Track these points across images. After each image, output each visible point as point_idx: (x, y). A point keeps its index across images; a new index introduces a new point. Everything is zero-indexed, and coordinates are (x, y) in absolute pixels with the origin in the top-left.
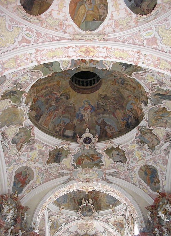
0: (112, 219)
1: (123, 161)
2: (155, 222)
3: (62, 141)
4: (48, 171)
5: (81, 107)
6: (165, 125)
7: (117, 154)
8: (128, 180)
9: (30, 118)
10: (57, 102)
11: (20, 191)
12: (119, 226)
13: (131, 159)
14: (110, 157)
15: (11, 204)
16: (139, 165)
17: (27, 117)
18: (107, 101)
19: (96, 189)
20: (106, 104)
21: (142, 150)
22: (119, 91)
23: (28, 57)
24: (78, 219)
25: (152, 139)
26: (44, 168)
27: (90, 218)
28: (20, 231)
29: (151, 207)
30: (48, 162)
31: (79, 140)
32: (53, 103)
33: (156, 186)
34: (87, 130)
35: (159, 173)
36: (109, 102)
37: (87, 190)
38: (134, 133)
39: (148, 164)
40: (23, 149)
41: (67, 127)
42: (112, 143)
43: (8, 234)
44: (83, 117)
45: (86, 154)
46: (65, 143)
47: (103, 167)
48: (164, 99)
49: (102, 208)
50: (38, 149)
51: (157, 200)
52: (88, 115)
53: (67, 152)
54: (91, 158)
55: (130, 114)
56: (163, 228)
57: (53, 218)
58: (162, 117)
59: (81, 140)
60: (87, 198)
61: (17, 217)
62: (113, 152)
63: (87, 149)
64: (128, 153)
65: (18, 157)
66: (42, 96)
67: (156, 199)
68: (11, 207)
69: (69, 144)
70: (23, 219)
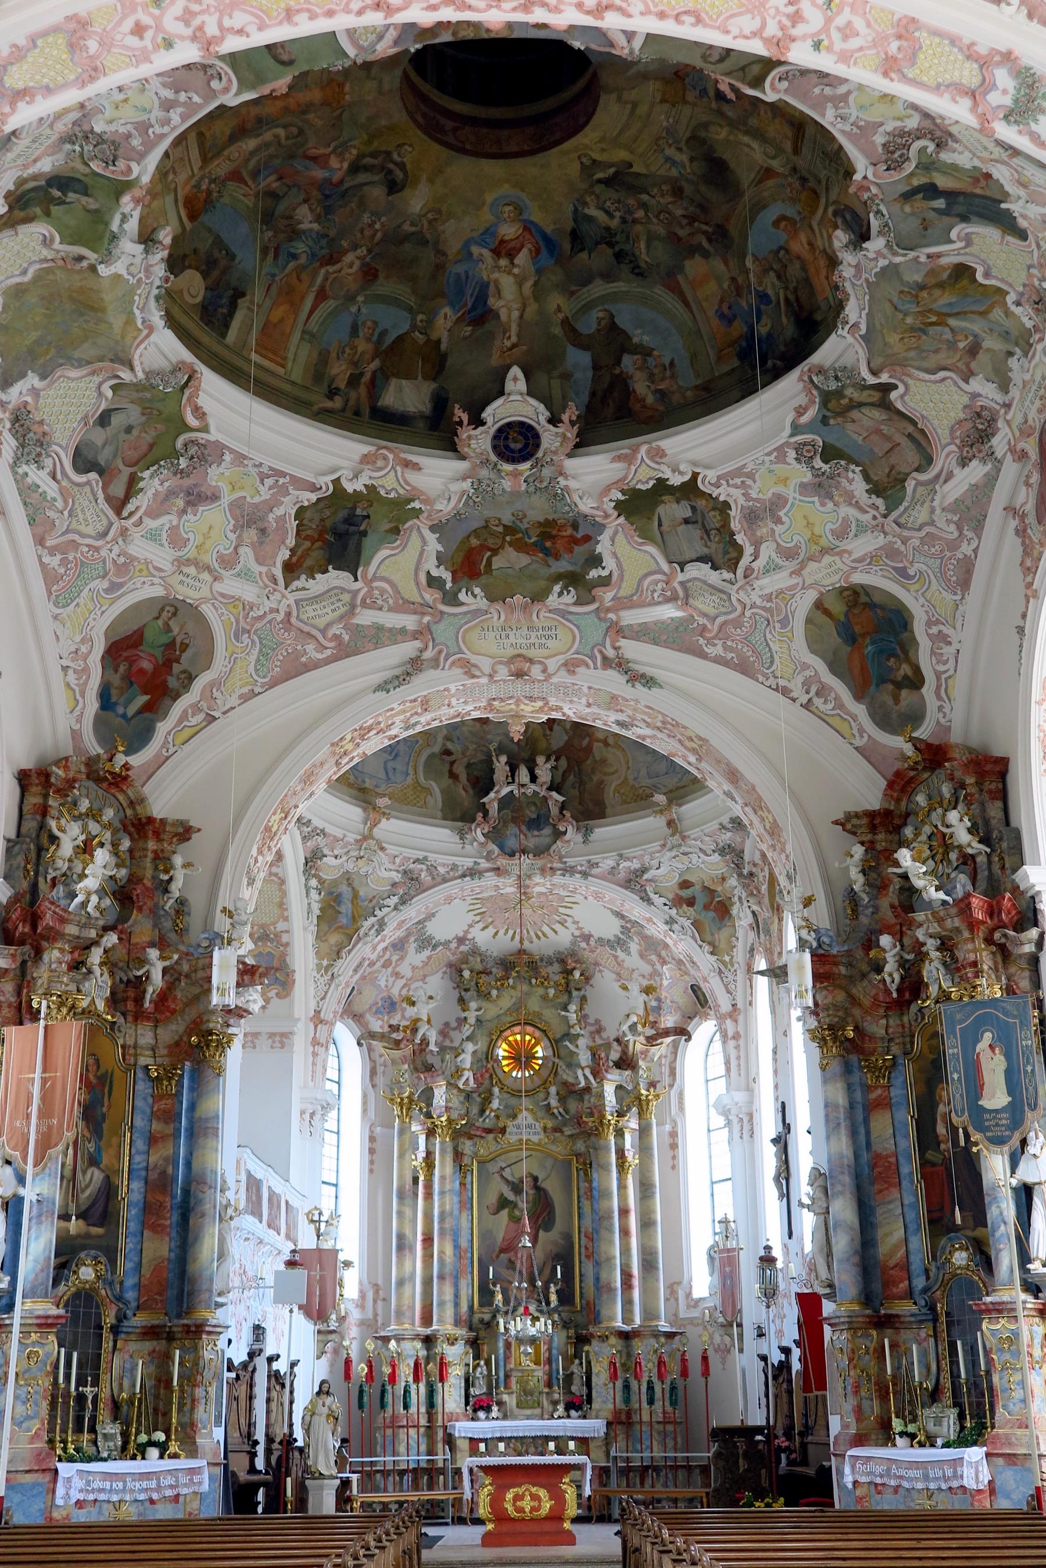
0: (667, 870)
1: (719, 559)
2: (885, 903)
3: (365, 449)
4: (293, 620)
5: (475, 234)
6: (968, 365)
7: (686, 521)
8: (744, 668)
9: (172, 322)
10: (328, 210)
11: (139, 739)
12: (706, 907)
13: (767, 551)
14: (646, 536)
15: (94, 814)
16: (811, 586)
17: (157, 318)
18: (631, 202)
19: (570, 713)
20: (624, 221)
21: (831, 498)
22: (703, 142)
23: (146, 20)
24: (472, 873)
25: (888, 438)
26: (268, 605)
27: (539, 863)
28: (153, 954)
29: (865, 821)
30: (291, 569)
31: (469, 437)
32: (306, 219)
33: (903, 703)
34: (515, 379)
35: (919, 629)
36: (644, 206)
37: (517, 716)
38: (784, 399)
39: (859, 578)
40: (140, 502)
41: (395, 357)
42: (658, 454)
43: (90, 972)
44: (492, 302)
45: (507, 518)
46: (385, 458)
47: (607, 596)
48: (964, 218)
49: (608, 811)
50: (226, 500)
51: (901, 784)
52: (520, 282)
53: (400, 512)
54: (535, 544)
55: (771, 285)
56: (920, 934)
57: (331, 866)
58: (950, 315)
59: (478, 441)
60: (525, 752)
61: (133, 879)
62: (661, 510)
63: (512, 493)
64: (752, 517)
65: (116, 550)
66: (235, 176)
67: (898, 774)
68: (94, 827)
69: (407, 464)
70: (165, 888)
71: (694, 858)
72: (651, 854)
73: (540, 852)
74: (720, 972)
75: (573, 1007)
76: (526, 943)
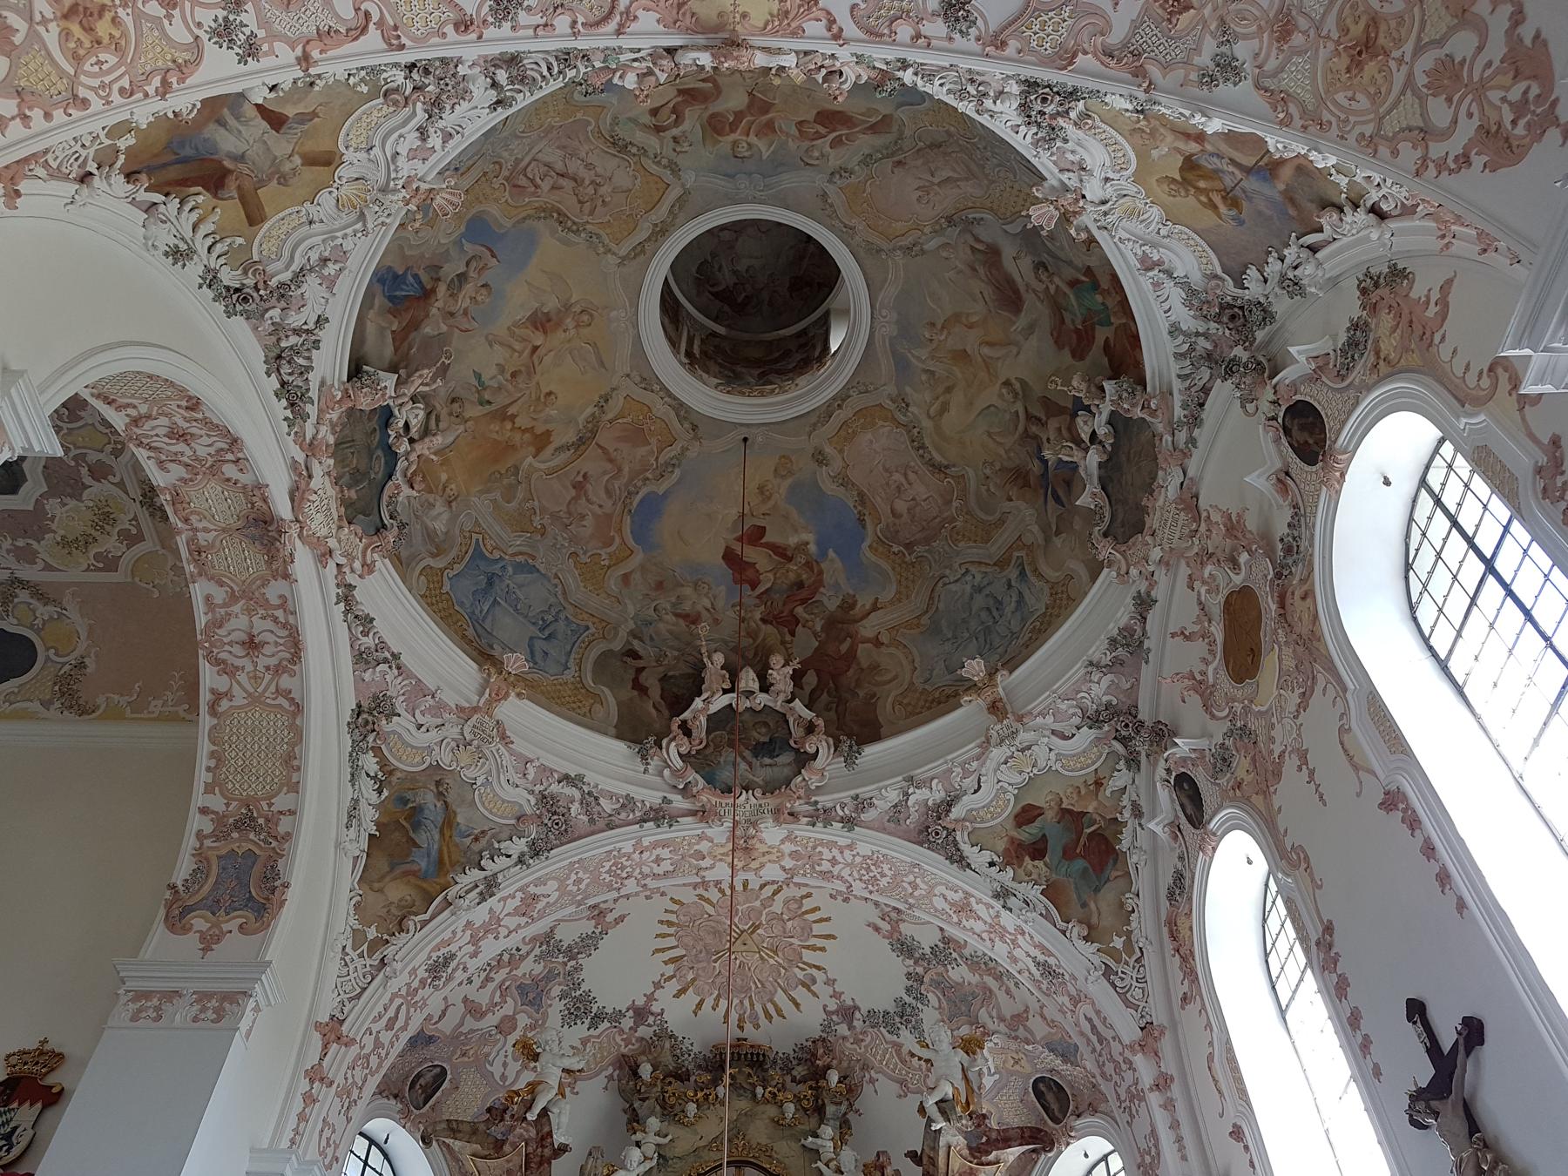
0: (992, 790)
12: (1068, 854)
24: (659, 816)
27: (771, 802)
71: (1040, 752)
72: (962, 765)
73: (769, 788)
74: (1108, 972)
75: (827, 1131)
76: (748, 1026)
